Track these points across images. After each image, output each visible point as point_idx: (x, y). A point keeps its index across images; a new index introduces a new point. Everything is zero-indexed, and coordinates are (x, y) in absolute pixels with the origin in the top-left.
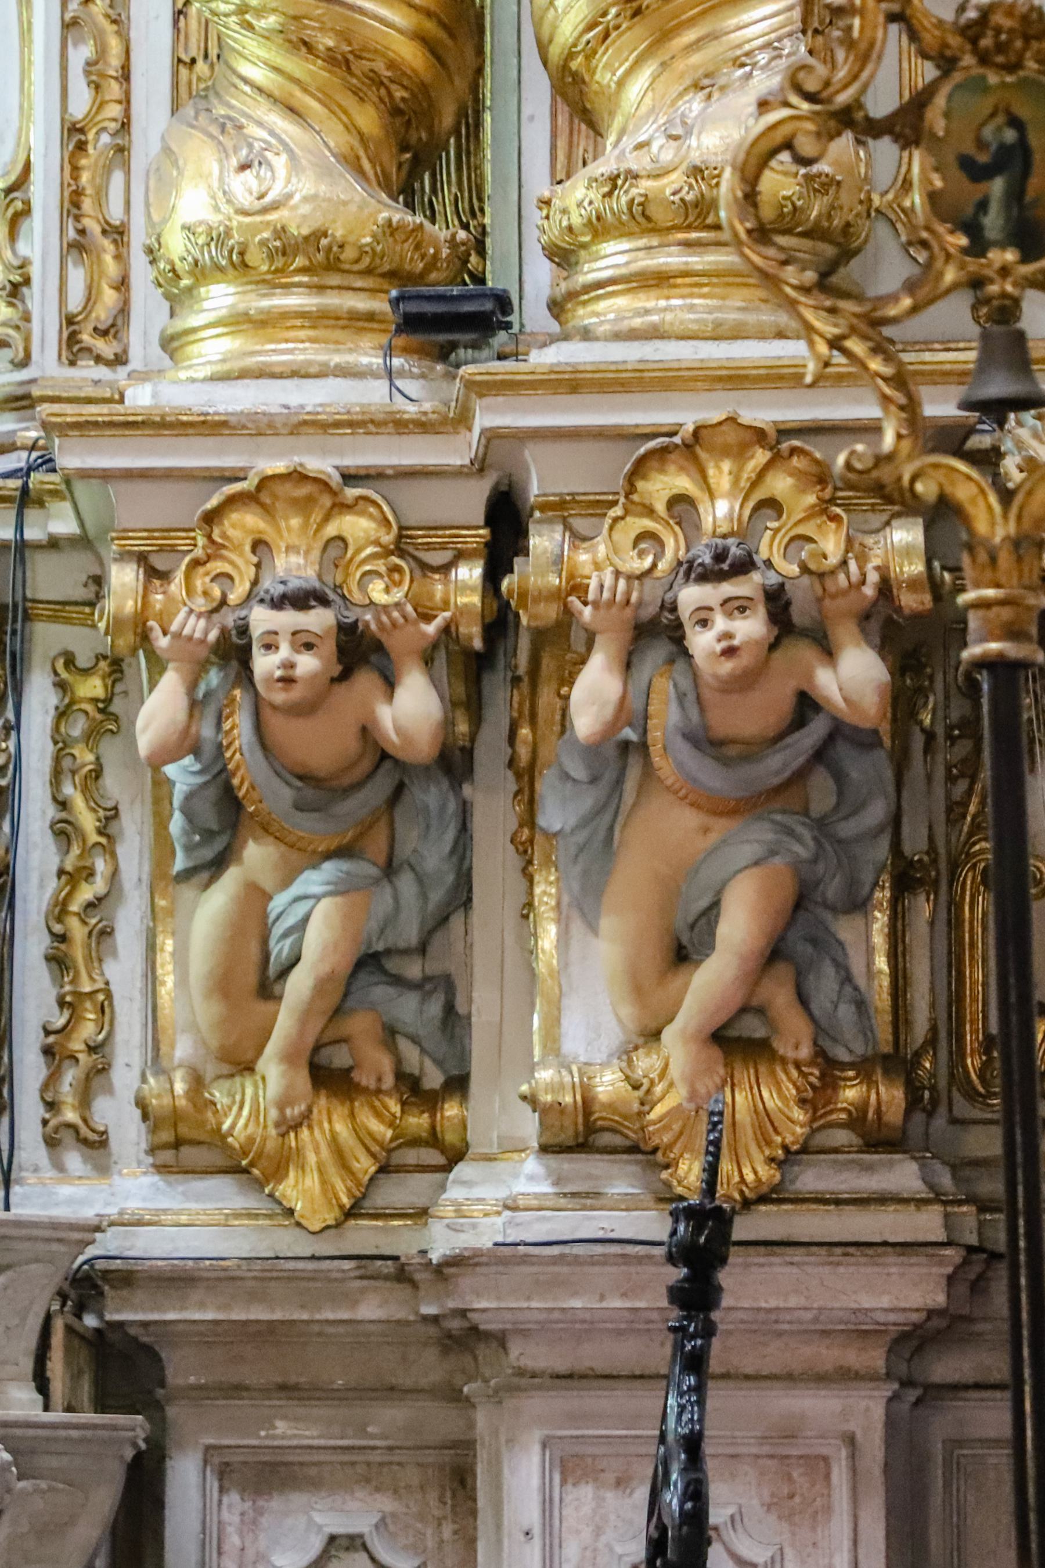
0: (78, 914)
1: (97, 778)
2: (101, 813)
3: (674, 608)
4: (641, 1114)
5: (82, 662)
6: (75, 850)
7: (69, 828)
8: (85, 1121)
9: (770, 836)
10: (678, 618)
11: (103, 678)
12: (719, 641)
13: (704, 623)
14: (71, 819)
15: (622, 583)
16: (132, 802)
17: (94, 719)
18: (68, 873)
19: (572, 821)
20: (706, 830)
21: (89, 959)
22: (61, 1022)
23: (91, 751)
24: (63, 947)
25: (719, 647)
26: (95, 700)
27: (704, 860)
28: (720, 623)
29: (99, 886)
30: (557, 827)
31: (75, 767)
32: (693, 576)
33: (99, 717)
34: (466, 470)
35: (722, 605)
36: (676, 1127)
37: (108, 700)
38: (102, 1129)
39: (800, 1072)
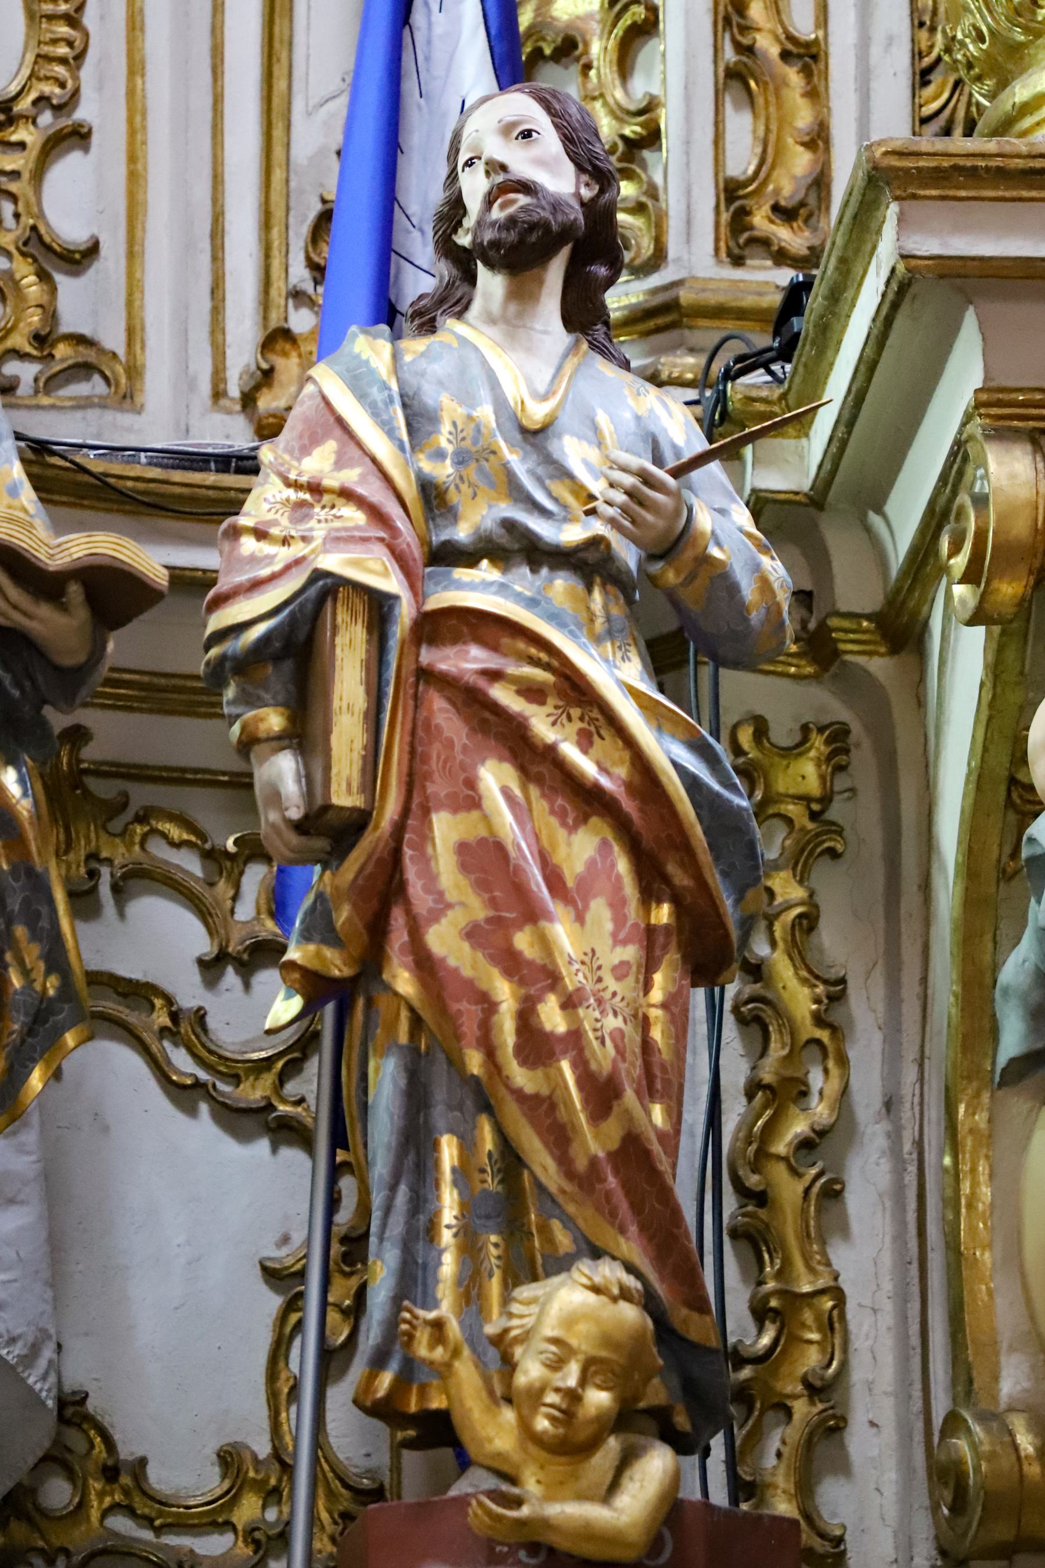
0: (785, 1159)
1: (811, 928)
2: (820, 989)
5: (782, 733)
6: (777, 1050)
7: (769, 1011)
8: (808, 1518)
11: (818, 766)
14: (769, 995)
16: (868, 974)
17: (803, 829)
18: (768, 1087)
21: (805, 1236)
22: (766, 1340)
23: (801, 882)
24: (762, 1213)
26: (805, 799)
29: (820, 1111)
31: (770, 911)
33: (810, 826)
37: (826, 799)
38: (838, 1532)
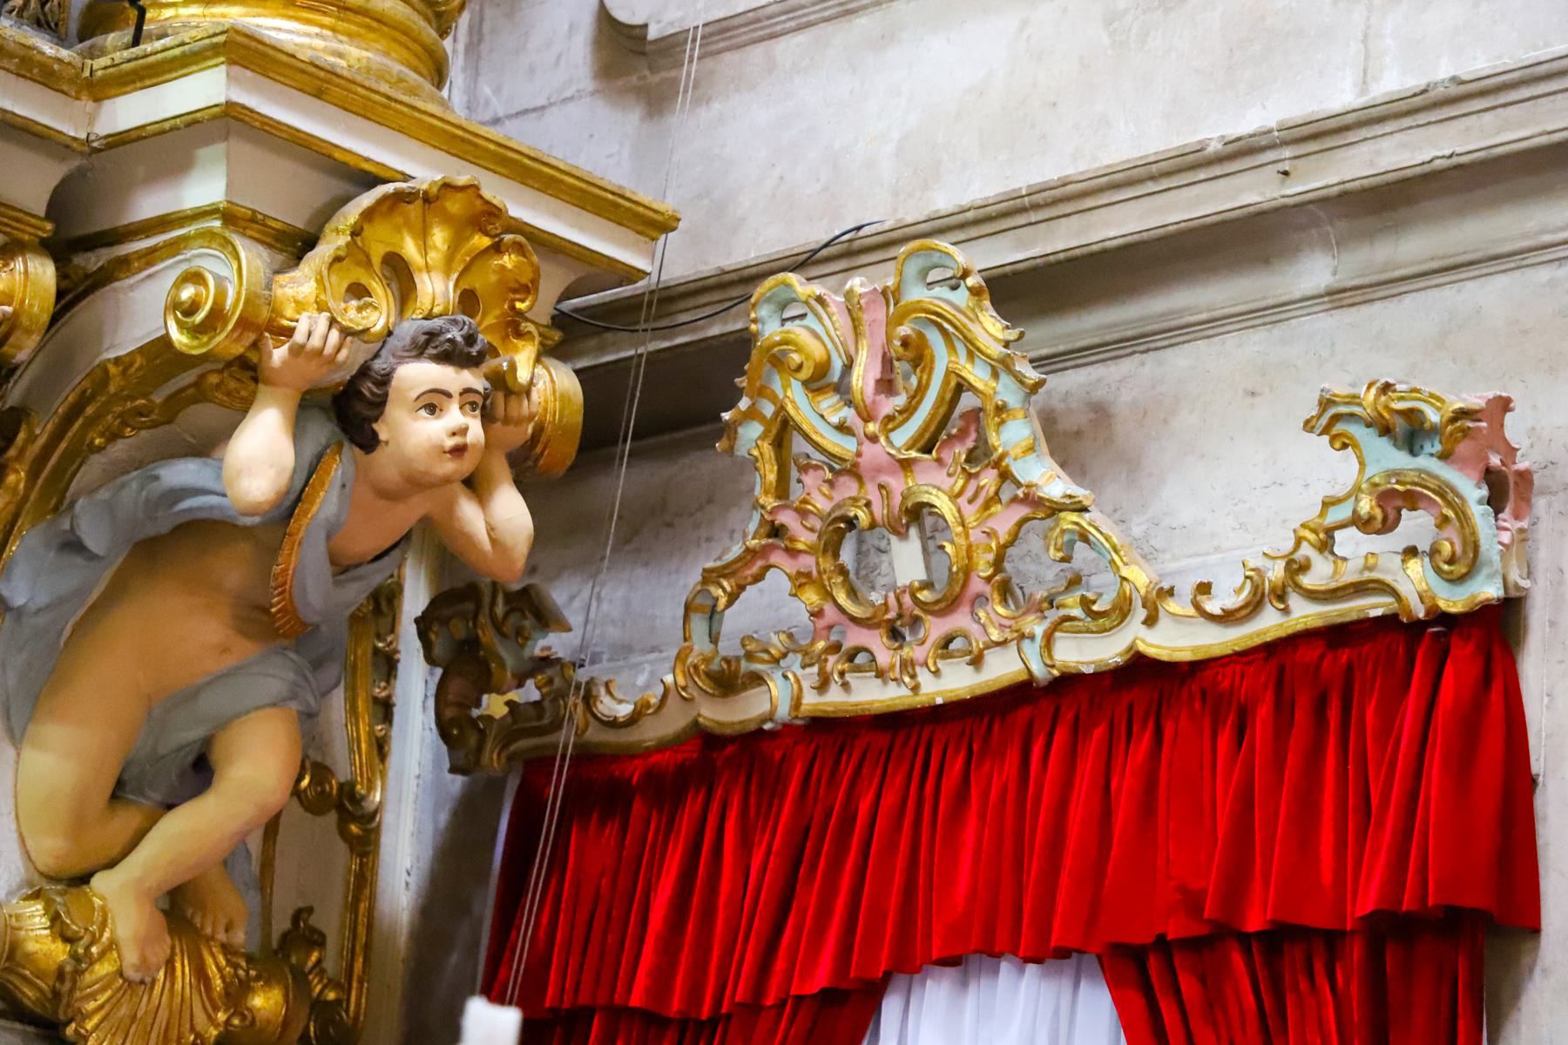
3: (385, 380)
4: (78, 972)
9: (291, 676)
10: (386, 395)
12: (454, 434)
13: (432, 409)
15: (334, 336)
19: (42, 599)
20: (225, 650)
25: (450, 443)
27: (210, 683)
28: (454, 416)
30: (19, 601)
32: (431, 351)
34: (75, 145)
35: (461, 394)
36: (102, 999)
39: (228, 961)
